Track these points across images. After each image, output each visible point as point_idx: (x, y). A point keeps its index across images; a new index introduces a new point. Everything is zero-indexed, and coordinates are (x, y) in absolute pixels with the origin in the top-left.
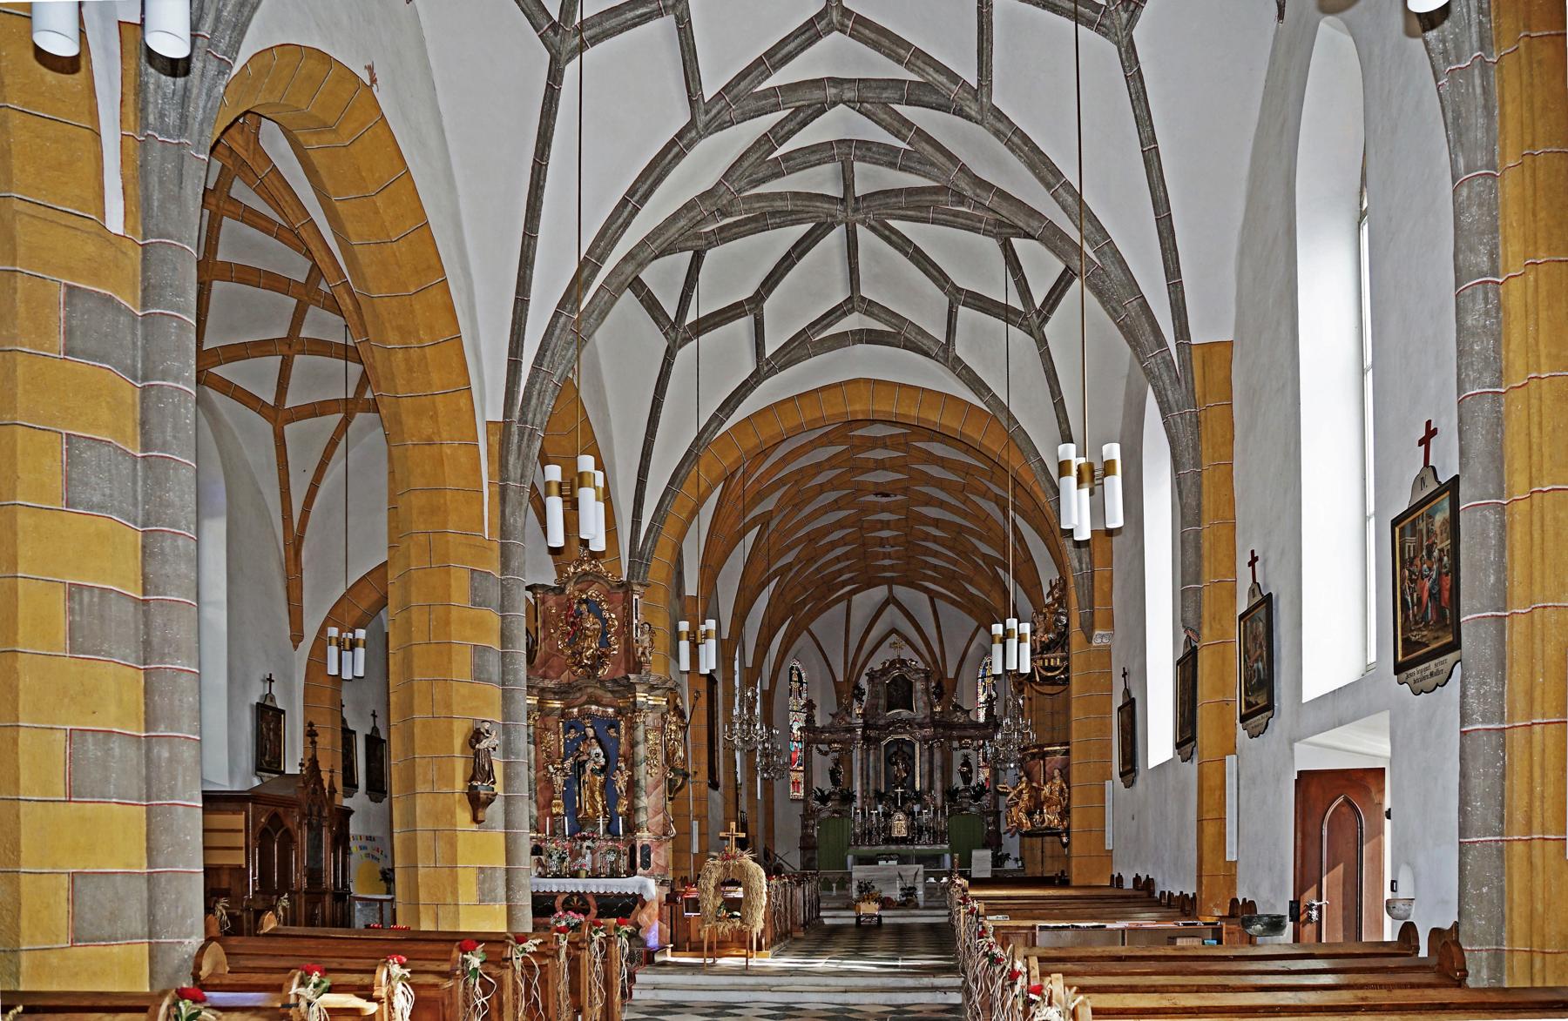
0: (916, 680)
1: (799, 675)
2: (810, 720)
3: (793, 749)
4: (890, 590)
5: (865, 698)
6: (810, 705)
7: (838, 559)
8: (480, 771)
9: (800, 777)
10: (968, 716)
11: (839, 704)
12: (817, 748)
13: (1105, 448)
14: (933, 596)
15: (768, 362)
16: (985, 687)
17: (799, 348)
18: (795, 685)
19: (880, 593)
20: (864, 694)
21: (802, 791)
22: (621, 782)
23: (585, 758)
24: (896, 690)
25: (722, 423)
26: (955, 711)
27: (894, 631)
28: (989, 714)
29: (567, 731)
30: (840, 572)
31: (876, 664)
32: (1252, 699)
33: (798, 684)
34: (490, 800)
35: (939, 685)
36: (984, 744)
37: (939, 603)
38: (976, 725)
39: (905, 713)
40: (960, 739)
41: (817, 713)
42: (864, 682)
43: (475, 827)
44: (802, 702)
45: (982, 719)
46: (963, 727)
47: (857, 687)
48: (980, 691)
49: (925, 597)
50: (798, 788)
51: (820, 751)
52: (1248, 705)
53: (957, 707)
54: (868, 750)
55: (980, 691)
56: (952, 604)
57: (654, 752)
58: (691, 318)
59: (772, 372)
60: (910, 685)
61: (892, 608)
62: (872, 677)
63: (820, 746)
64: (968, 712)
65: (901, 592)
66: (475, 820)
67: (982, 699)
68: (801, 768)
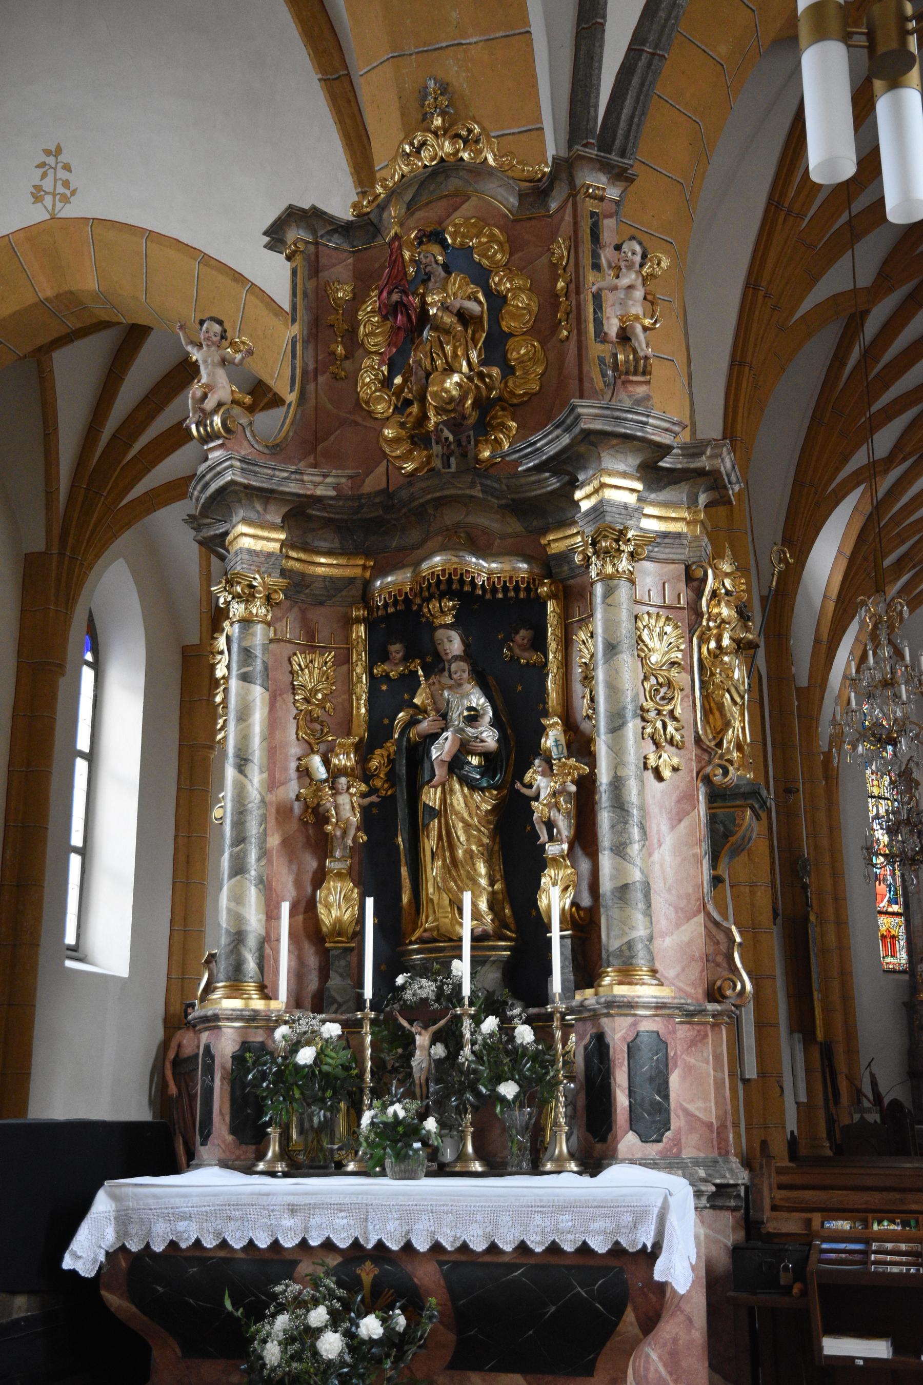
23: (425, 726)
29: (377, 654)
50: (893, 946)
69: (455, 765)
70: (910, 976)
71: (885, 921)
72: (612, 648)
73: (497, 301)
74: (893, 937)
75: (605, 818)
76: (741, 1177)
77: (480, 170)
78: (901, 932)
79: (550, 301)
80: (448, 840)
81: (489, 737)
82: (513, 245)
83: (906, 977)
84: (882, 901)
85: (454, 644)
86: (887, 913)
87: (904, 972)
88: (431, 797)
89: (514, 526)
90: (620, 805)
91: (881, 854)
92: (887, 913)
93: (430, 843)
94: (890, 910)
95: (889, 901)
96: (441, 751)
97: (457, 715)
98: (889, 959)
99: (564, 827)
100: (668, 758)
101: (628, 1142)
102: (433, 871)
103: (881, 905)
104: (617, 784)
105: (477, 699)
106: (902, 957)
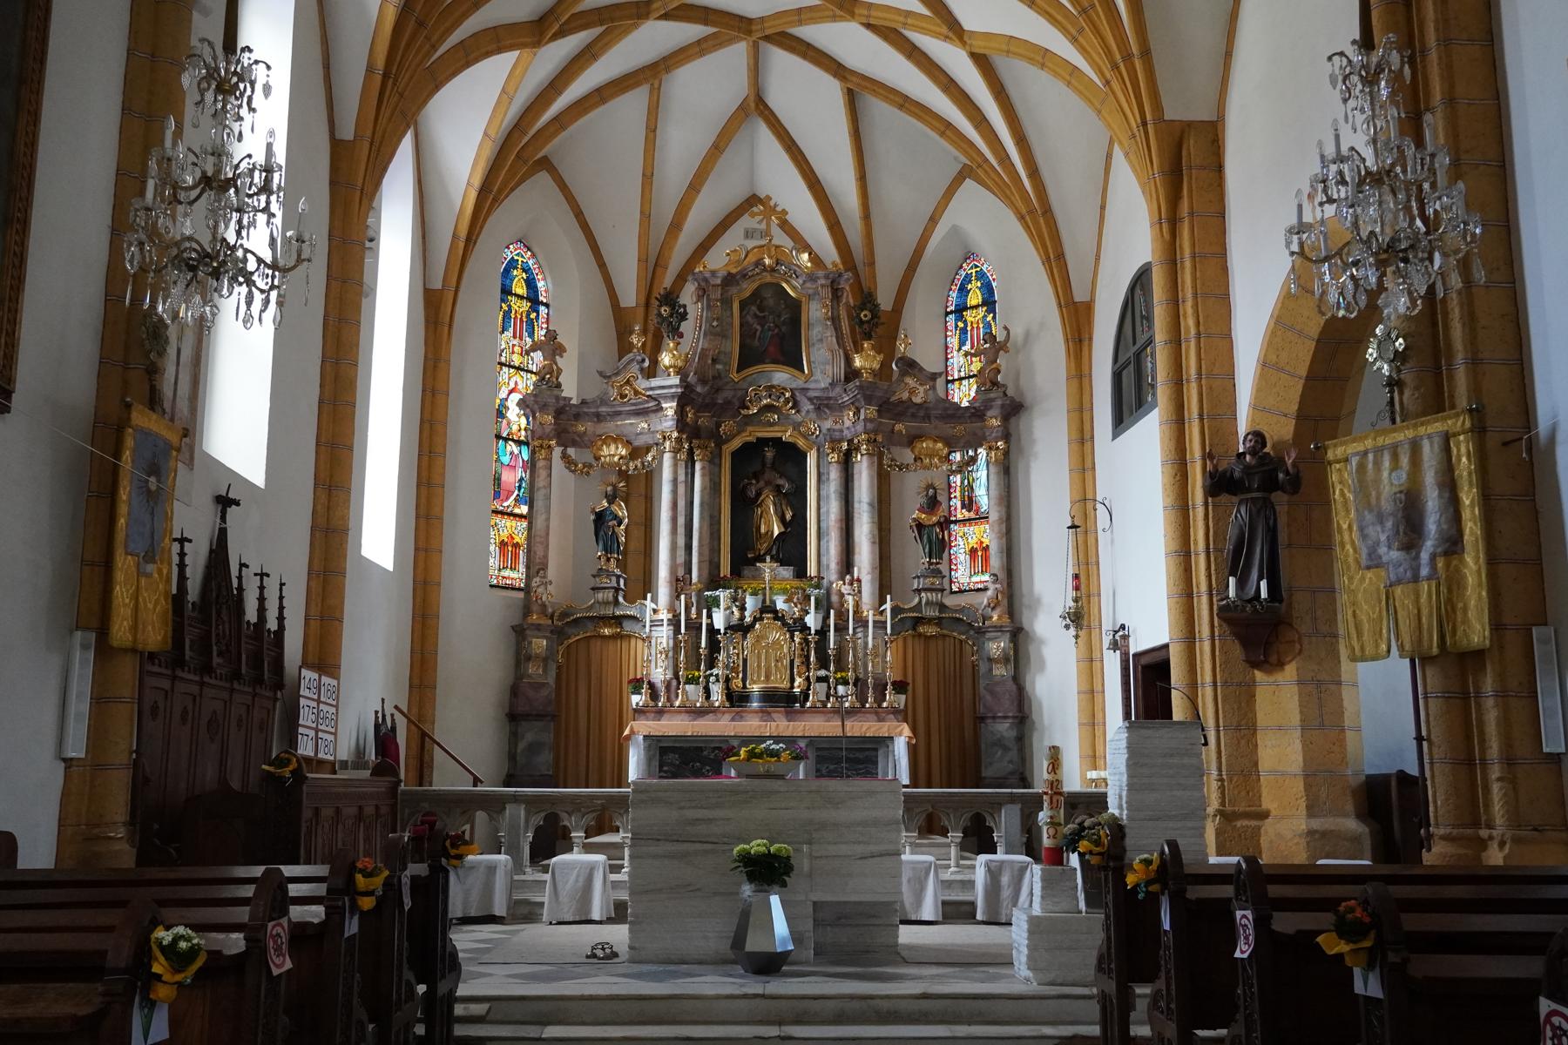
0: (810, 297)
1: (531, 284)
2: (548, 379)
3: (506, 459)
5: (686, 327)
10: (933, 388)
11: (624, 348)
12: (564, 456)
16: (964, 331)
18: (519, 307)
20: (683, 317)
21: (522, 568)
24: (762, 321)
26: (903, 374)
28: (989, 381)
31: (717, 260)
33: (526, 305)
37: (879, 111)
38: (953, 413)
39: (781, 376)
40: (911, 440)
42: (688, 296)
46: (922, 412)
47: (670, 298)
48: (954, 341)
49: (832, 89)
50: (515, 556)
53: (910, 366)
54: (691, 462)
55: (954, 341)
56: (901, 107)
60: (795, 307)
61: (764, 137)
63: (571, 451)
64: (934, 377)
68: (524, 509)
70: (526, 593)
71: (508, 524)
74: (517, 546)
78: (520, 538)
83: (521, 595)
84: (507, 499)
86: (511, 514)
87: (519, 589)
91: (513, 440)
92: (511, 514)
94: (517, 511)
95: (516, 500)
98: (507, 573)
103: (505, 504)
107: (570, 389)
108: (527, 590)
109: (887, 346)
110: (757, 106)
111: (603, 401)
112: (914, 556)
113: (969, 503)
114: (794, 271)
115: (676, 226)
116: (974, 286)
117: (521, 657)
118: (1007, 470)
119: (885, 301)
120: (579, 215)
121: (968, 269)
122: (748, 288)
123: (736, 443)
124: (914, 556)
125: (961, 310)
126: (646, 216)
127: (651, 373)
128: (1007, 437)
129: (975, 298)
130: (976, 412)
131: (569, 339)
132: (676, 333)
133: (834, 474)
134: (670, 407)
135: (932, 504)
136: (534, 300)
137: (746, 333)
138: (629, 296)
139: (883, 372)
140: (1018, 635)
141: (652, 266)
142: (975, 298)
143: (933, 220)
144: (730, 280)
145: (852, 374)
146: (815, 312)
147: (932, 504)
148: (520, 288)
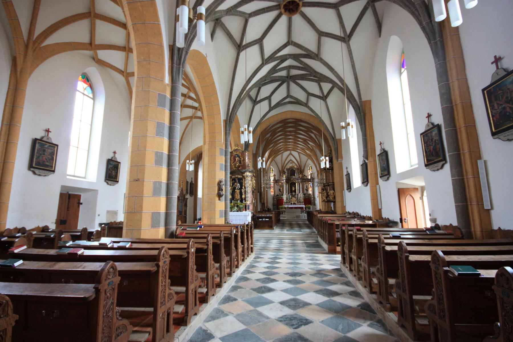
2: (275, 178)
4: (290, 152)
6: (274, 175)
7: (281, 146)
8: (220, 189)
9: (273, 190)
11: (280, 175)
13: (341, 123)
14: (299, 153)
15: (272, 108)
17: (279, 104)
18: (271, 171)
19: (288, 152)
22: (243, 191)
25: (263, 119)
27: (291, 160)
28: (311, 177)
29: (232, 181)
30: (281, 148)
31: (288, 167)
32: (383, 173)
34: (222, 195)
35: (301, 171)
36: (310, 183)
37: (300, 154)
38: (308, 179)
39: (294, 177)
40: (305, 182)
41: (276, 177)
42: (285, 170)
43: (219, 201)
44: (273, 175)
45: (309, 178)
47: (284, 171)
49: (297, 153)
51: (277, 185)
52: (381, 174)
53: (305, 176)
55: (309, 172)
57: (250, 185)
58: (258, 99)
59: (272, 110)
60: (295, 171)
61: (291, 156)
62: (287, 169)
65: (293, 153)
66: (219, 200)
67: (309, 173)
69: (238, 189)
72: (247, 183)
73: (240, 159)
75: (246, 193)
76: (253, 212)
77: (239, 149)
79: (244, 159)
80: (237, 193)
81: (239, 187)
82: (241, 155)
85: (237, 181)
88: (236, 191)
89: (241, 173)
90: (247, 192)
93: (236, 193)
96: (237, 188)
97: (238, 186)
99: (244, 193)
100: (250, 189)
101: (247, 210)
102: (236, 195)
104: (247, 191)
105: (239, 185)
106: (273, 194)
107: (276, 179)
108: (274, 195)
109: (303, 174)
110: (291, 154)
111: (279, 179)
112: (305, 192)
113: (310, 186)
114: (294, 167)
115: (284, 163)
116: (310, 167)
117: (274, 200)
118: (313, 184)
119: (302, 169)
120: (276, 163)
121: (310, 166)
122: (291, 169)
123: (290, 183)
124: (305, 192)
125: (309, 169)
126: (282, 163)
127: (283, 177)
128: (313, 181)
129: (310, 168)
130: (310, 179)
131: (276, 174)
132: (285, 174)
133: (298, 185)
134: (285, 181)
135: (307, 187)
136: (273, 171)
137: (291, 173)
138: (280, 169)
139: (302, 177)
140: (314, 198)
141: (282, 167)
142: (310, 168)
143: (307, 161)
144: (289, 169)
145: (300, 177)
146: (296, 171)
147: (307, 187)
148: (271, 170)
